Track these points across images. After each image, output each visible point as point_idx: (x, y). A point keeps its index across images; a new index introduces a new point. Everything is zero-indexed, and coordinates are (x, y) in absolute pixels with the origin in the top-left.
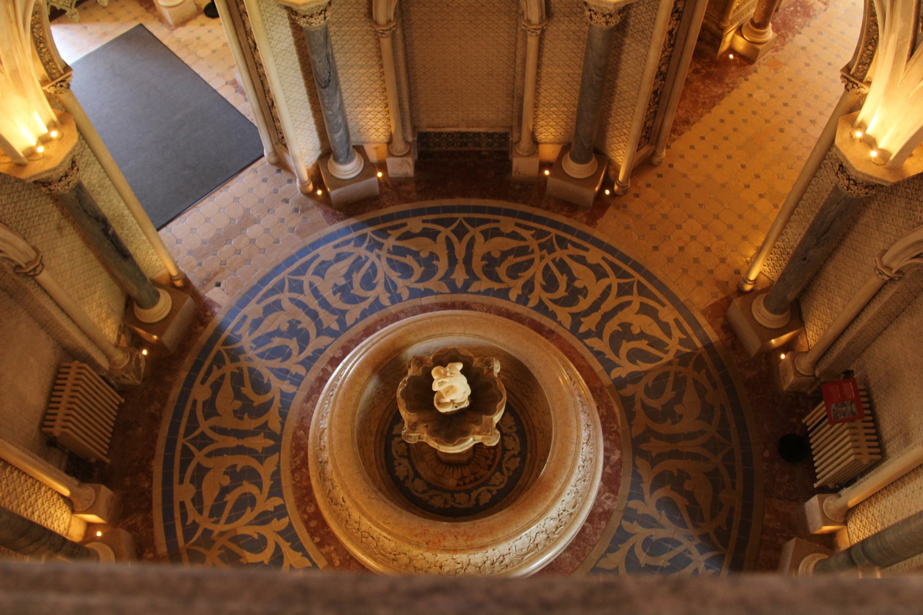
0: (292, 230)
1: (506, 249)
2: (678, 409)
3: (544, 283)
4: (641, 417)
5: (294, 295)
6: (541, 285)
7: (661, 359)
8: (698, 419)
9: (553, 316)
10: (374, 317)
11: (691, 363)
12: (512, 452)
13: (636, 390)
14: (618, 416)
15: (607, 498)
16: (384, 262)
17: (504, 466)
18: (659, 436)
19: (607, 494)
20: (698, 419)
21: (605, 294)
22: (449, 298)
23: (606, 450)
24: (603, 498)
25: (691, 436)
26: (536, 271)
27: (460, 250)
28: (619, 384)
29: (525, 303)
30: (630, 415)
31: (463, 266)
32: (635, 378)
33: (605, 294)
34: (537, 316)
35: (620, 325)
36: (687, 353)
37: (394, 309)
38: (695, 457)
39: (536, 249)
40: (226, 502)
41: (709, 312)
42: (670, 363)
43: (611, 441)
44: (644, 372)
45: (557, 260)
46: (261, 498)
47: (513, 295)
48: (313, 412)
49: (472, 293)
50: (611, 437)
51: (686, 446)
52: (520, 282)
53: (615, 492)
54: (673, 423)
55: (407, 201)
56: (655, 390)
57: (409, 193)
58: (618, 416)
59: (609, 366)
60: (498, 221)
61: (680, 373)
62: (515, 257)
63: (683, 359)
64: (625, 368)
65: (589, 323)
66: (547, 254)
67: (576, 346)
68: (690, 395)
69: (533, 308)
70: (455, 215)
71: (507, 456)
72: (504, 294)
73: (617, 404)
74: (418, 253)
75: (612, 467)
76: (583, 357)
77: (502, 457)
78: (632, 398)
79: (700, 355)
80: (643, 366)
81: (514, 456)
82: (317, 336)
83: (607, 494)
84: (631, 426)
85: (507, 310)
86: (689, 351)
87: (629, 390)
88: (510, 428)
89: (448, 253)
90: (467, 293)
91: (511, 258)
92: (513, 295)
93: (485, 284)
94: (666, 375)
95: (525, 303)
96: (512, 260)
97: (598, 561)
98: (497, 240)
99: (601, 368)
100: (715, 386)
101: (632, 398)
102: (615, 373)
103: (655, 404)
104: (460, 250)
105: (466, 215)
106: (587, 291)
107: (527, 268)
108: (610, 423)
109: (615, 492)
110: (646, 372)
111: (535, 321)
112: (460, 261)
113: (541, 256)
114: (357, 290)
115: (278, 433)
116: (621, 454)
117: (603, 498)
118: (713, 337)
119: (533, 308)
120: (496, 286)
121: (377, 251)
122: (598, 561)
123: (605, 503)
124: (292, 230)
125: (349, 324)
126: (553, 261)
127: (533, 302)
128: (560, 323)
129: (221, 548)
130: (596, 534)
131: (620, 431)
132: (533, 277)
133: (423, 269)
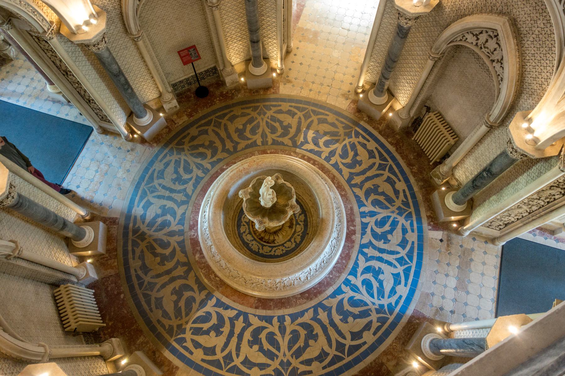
0: (433, 294)
1: (308, 349)
2: (175, 297)
3: (275, 337)
4: (191, 282)
5: (398, 256)
6: (276, 335)
7: (193, 323)
8: (163, 297)
9: (261, 318)
10: (351, 265)
11: (175, 329)
12: (246, 234)
13: (199, 297)
14: (204, 278)
15: (194, 235)
16: (368, 302)
17: (247, 226)
18: (180, 277)
19: (194, 237)
20: (163, 297)
21: (238, 349)
22: (321, 298)
23: (204, 257)
24: (196, 234)
25: (163, 286)
26: (284, 343)
27: (334, 335)
28: (209, 296)
29: (279, 317)
30: (198, 281)
31: (325, 323)
32: (203, 303)
33: (238, 349)
34: (269, 313)
35: (222, 332)
36: (179, 334)
37: (344, 276)
38: (158, 276)
39: (291, 360)
40: (352, 151)
41: (174, 370)
42: (187, 323)
43: (203, 263)
44: (199, 310)
45: (275, 358)
46: (339, 160)
47: (288, 319)
48: (344, 205)
49: (310, 308)
50: (203, 265)
51: (166, 278)
52: (288, 331)
53: (191, 239)
54: (175, 288)
55: (385, 353)
56: (190, 301)
57: (388, 360)
58: (204, 278)
59: (219, 304)
60: (324, 368)
61: (180, 320)
62: (300, 346)
63: (181, 329)
64: (209, 307)
65: (240, 324)
66: (283, 359)
67: (240, 306)
68: (169, 308)
69: (274, 317)
70: (351, 358)
71: (248, 231)
72: (294, 317)
73: (207, 284)
74: (354, 319)
75: (197, 250)
76: (234, 301)
77: (249, 228)
78: (200, 291)
79: (171, 336)
80: (201, 313)
81: (244, 232)
82: (370, 240)
83: (194, 237)
84: (196, 276)
85: (286, 308)
86: (179, 336)
87: (204, 294)
88: (253, 245)
89: (338, 328)
90: (313, 307)
91: (302, 344)
92: (288, 319)
93: (307, 318)
94: (187, 314)
95: (279, 317)
96: (301, 343)
97: (188, 207)
98: (316, 353)
99: (222, 300)
100: (159, 321)
101: (200, 291)
102: (214, 300)
103: (187, 294)
104: (334, 335)
105: (344, 362)
106: (249, 345)
107: (289, 342)
108: (206, 272)
109: (191, 239)
110: (198, 310)
111: (269, 310)
112: (328, 326)
113: (286, 356)
114: (369, 276)
115: (353, 188)
116: (195, 259)
117: (196, 234)
118: (167, 354)
119: (274, 317)
120: (300, 320)
121: (377, 307)
122: (188, 207)
123: (194, 232)
124: (433, 294)
125: (360, 255)
126: (277, 357)
127: (275, 320)
128: (255, 315)
129: (340, 135)
130: (193, 217)
131: (200, 270)
132: (283, 337)
133: (345, 309)
